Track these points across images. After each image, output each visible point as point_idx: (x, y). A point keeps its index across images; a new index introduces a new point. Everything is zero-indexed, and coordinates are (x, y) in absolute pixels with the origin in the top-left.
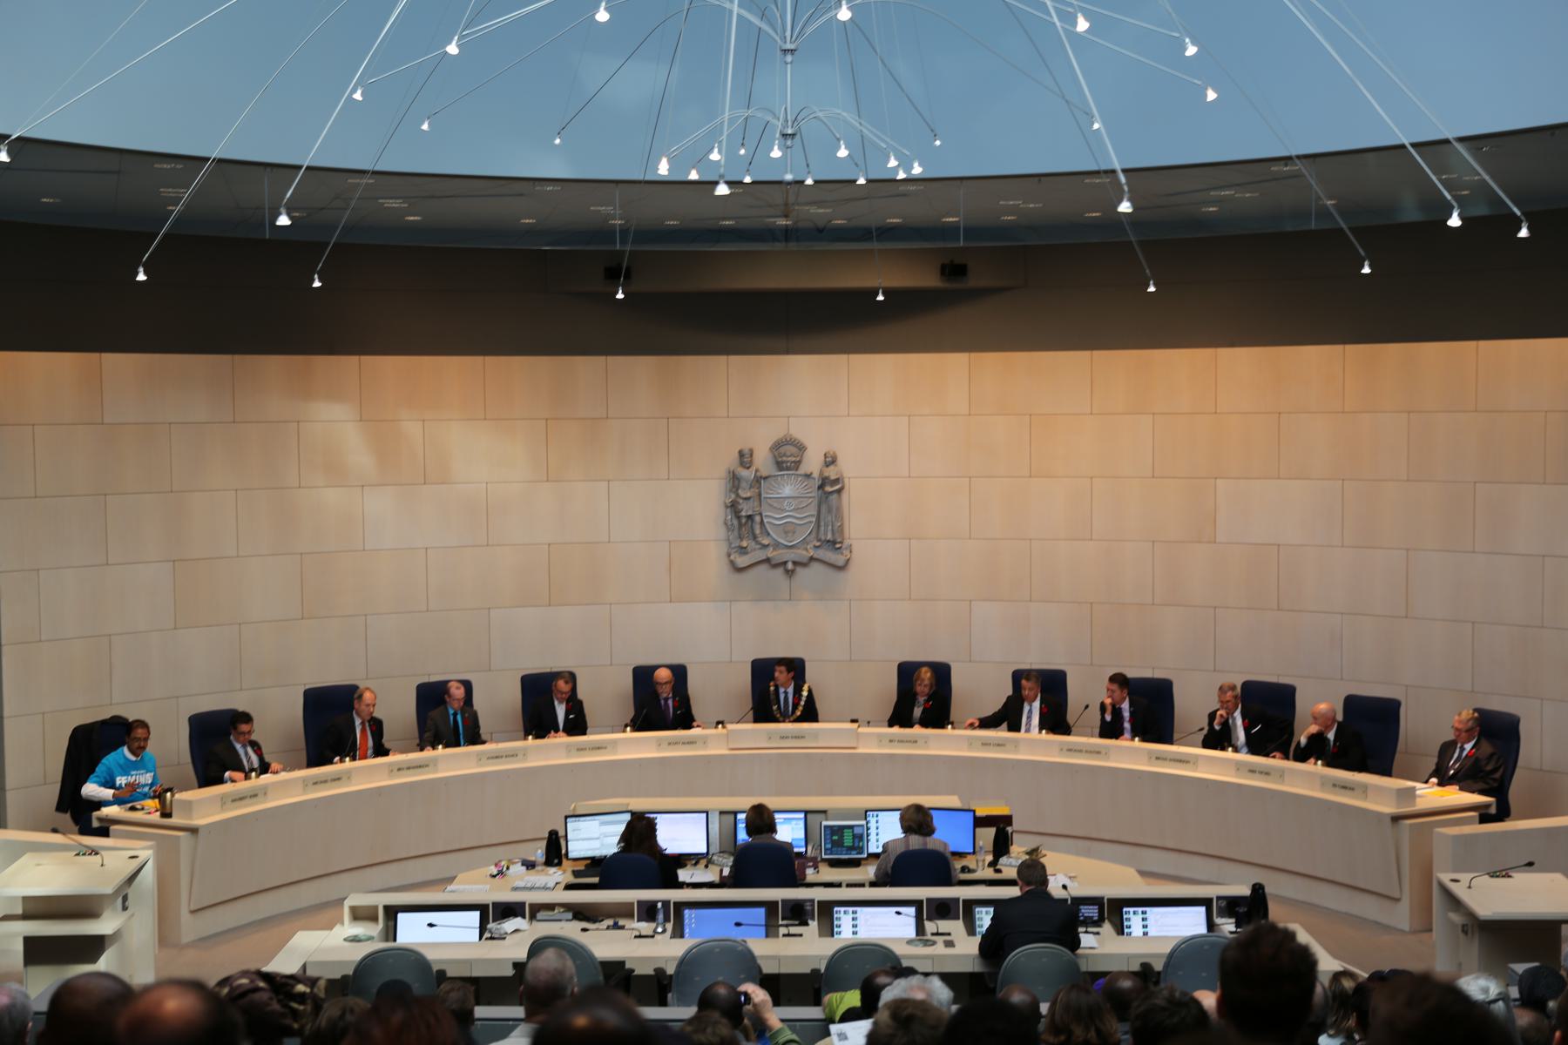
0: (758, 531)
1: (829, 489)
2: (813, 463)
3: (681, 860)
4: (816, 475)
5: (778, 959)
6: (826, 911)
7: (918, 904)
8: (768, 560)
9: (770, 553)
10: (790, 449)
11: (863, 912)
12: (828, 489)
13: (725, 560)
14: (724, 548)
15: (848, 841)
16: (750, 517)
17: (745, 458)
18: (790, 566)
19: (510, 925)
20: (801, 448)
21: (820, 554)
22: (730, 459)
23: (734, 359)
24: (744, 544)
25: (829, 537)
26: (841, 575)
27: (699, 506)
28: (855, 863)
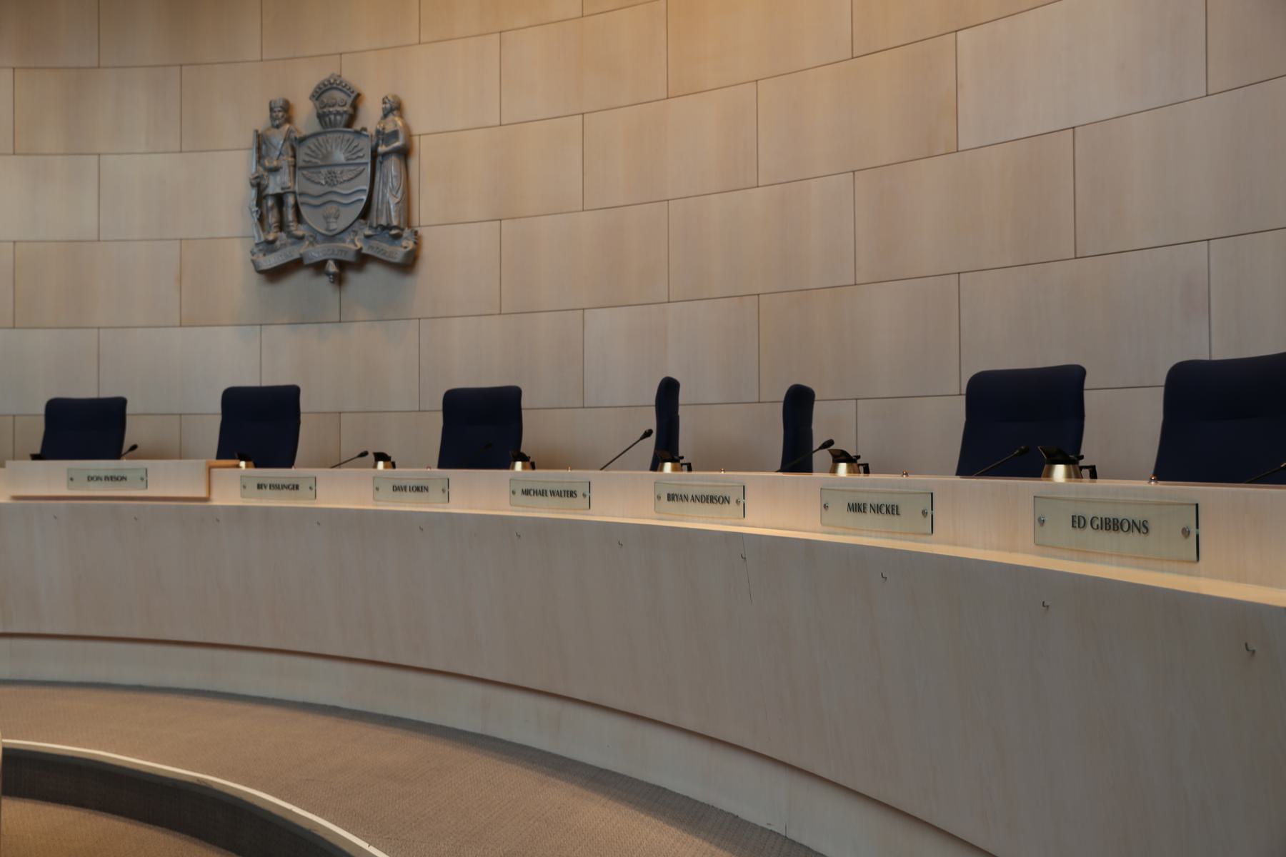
2: (371, 117)
10: (338, 96)
13: (251, 266)
16: (280, 199)
17: (282, 113)
22: (261, 119)
24: (271, 237)
26: (408, 281)
27: (220, 192)
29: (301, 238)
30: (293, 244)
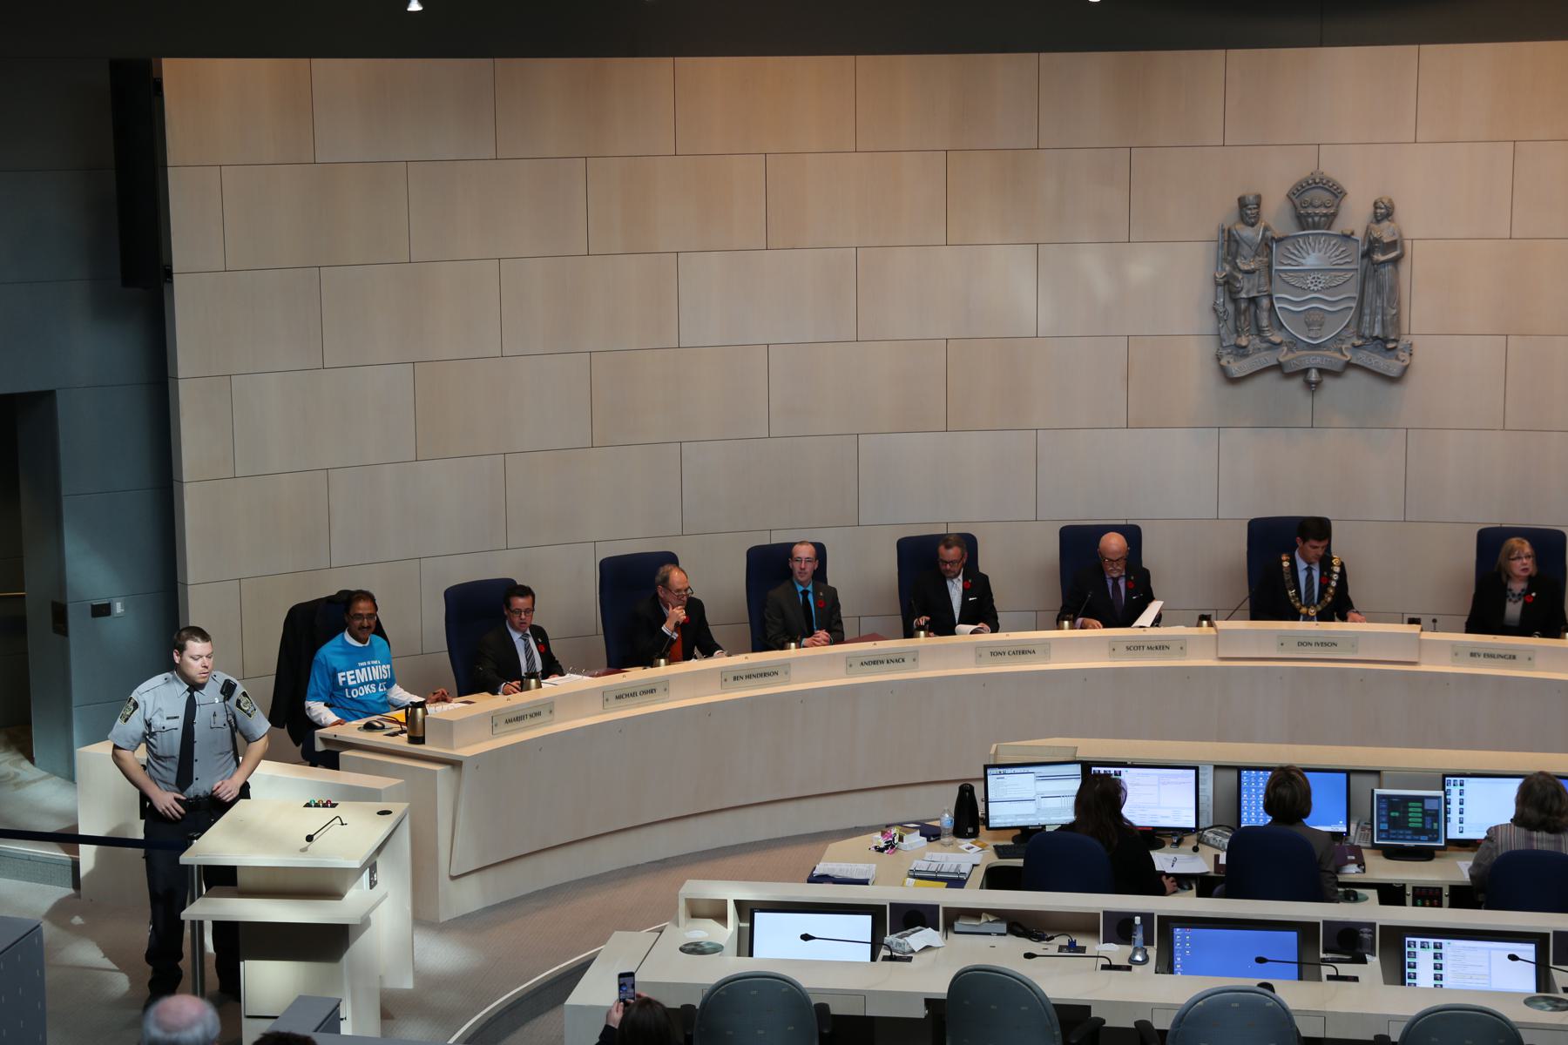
0: (1264, 322)
1: (1379, 258)
2: (1355, 216)
3: (1156, 837)
4: (1359, 235)
5: (1324, 1016)
6: (1395, 942)
7: (1539, 939)
8: (1279, 367)
9: (1283, 356)
11: (1451, 946)
12: (1379, 257)
13: (1213, 365)
14: (1211, 346)
15: (1415, 820)
17: (1248, 209)
18: (1313, 376)
19: (920, 938)
20: (1338, 193)
21: (1363, 358)
22: (1223, 211)
23: (1236, 55)
24: (1243, 341)
25: (1377, 331)
27: (1169, 282)
28: (1426, 854)
29: (1280, 344)
30: (1267, 349)
